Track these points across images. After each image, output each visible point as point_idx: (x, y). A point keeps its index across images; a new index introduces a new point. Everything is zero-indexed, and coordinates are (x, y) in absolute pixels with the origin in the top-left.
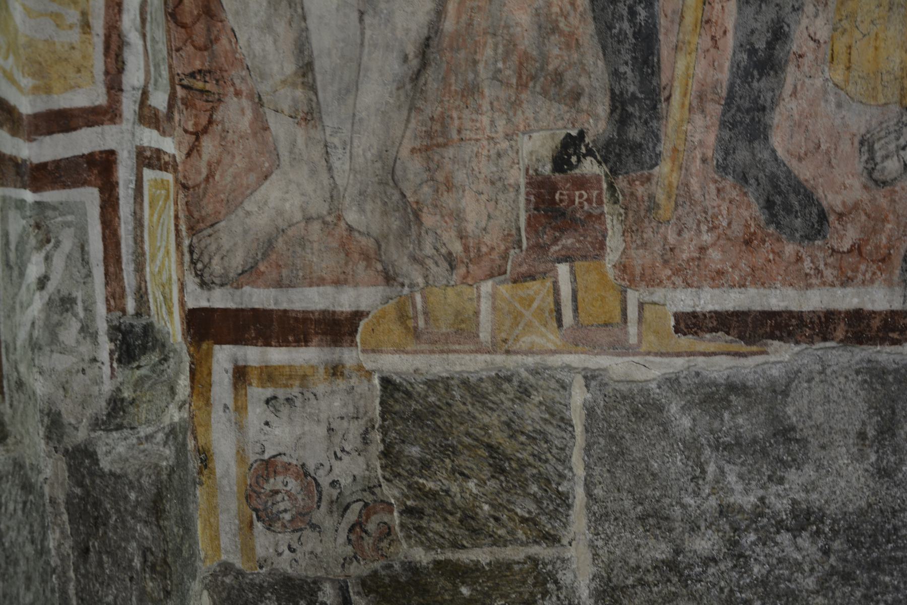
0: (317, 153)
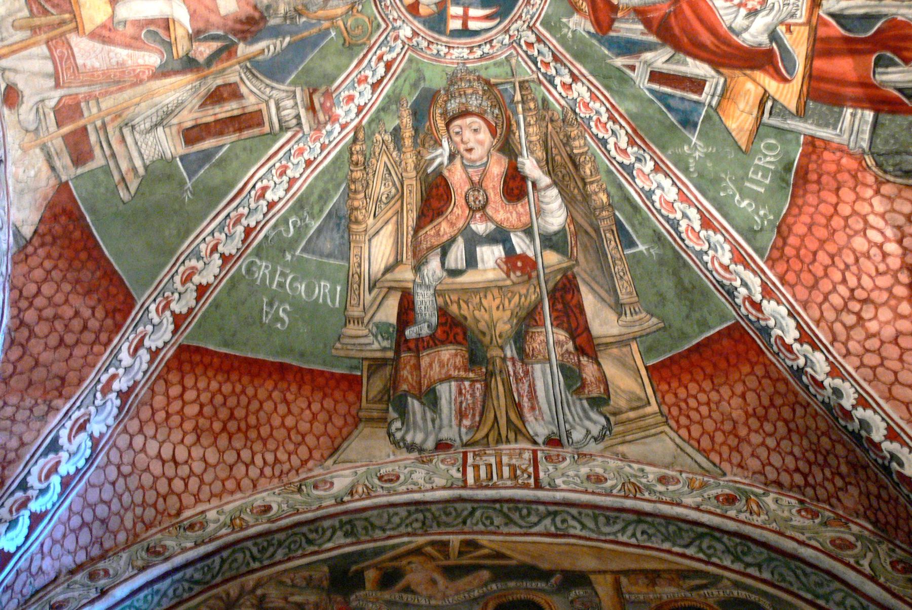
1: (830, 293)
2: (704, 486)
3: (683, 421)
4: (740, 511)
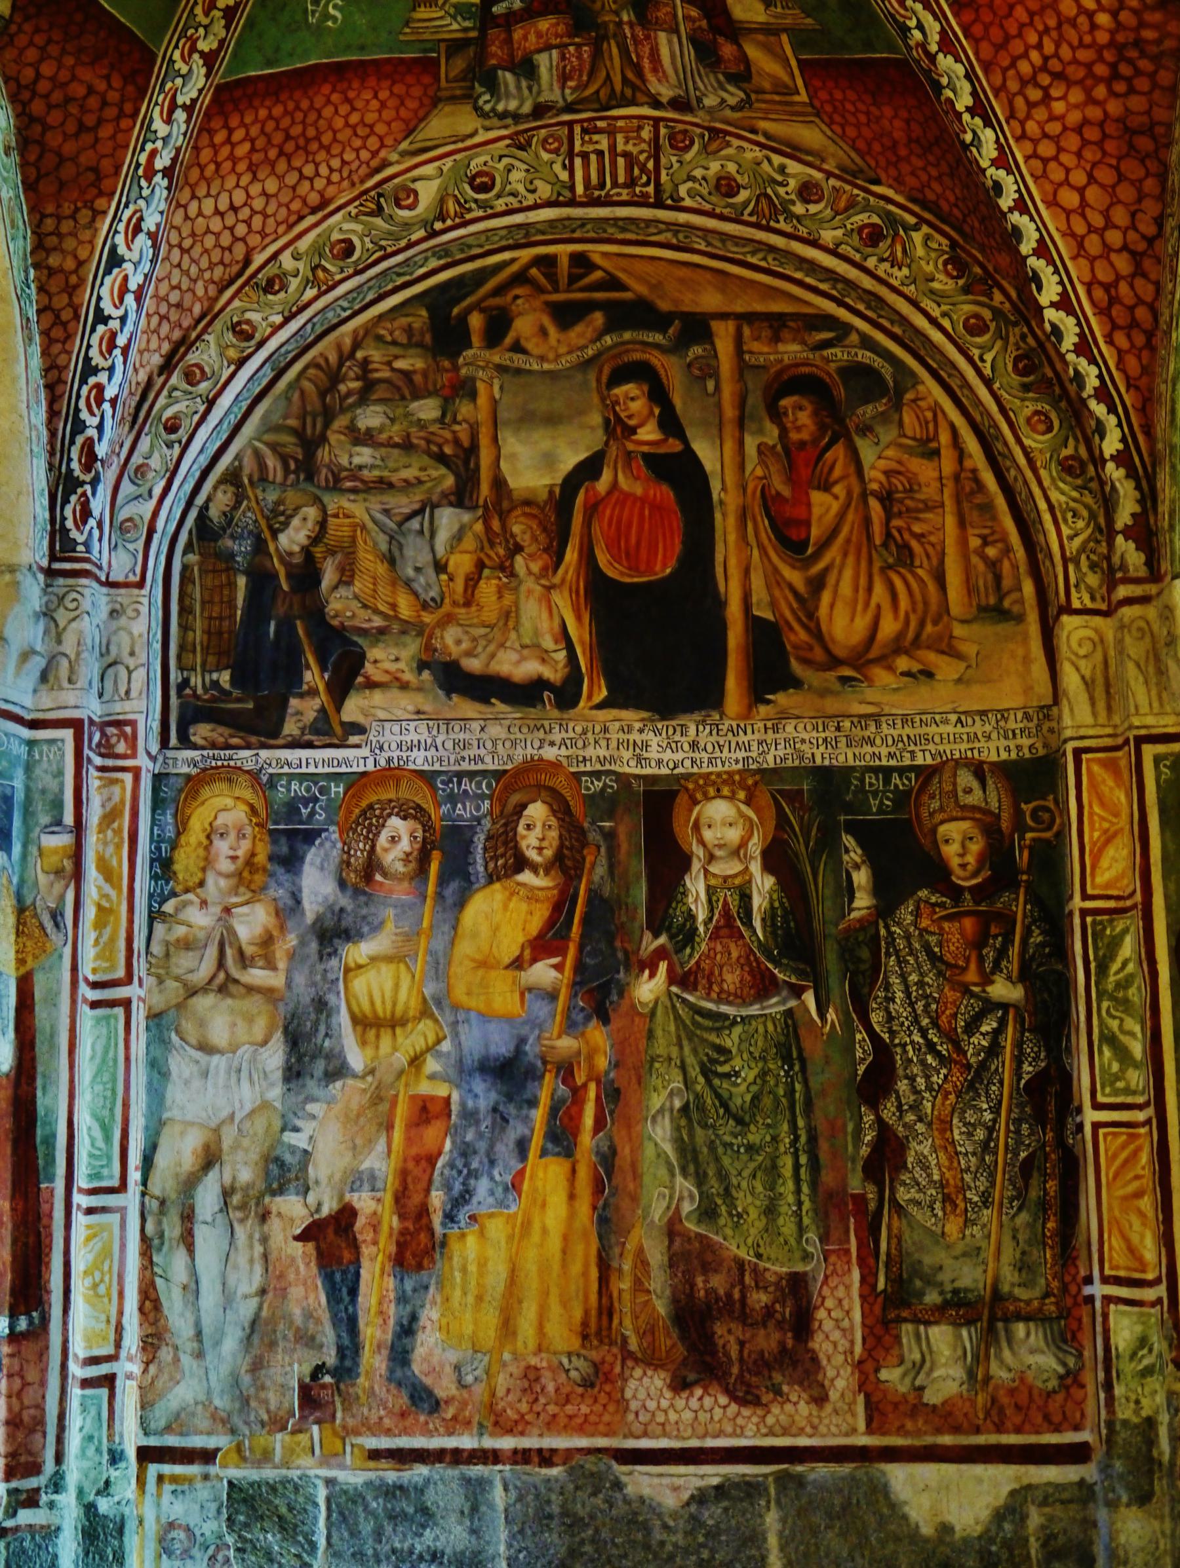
1: (1020, 57)
2: (852, 204)
3: (837, 118)
4: (882, 260)
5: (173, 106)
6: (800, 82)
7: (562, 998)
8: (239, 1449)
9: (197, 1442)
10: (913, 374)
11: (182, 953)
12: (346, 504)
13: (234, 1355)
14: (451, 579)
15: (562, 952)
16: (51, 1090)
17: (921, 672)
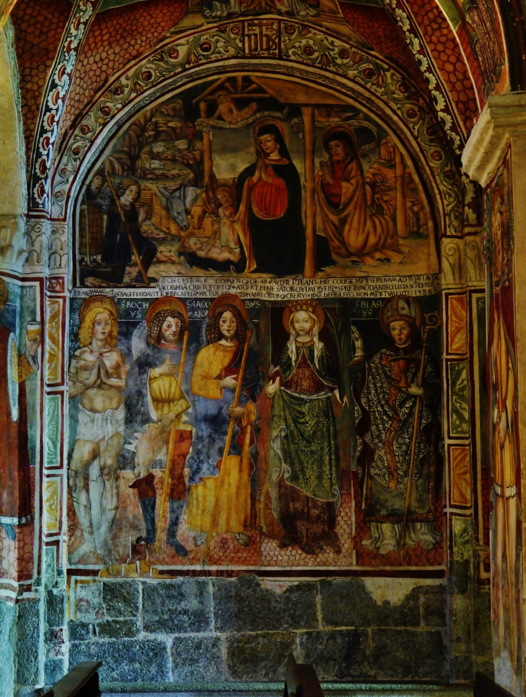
0: (92, 540)
4: (373, 84)
5: (79, 23)
6: (340, 10)
7: (237, 391)
8: (108, 570)
9: (91, 567)
10: (385, 131)
11: (83, 372)
12: (149, 185)
13: (105, 533)
14: (192, 217)
15: (237, 373)
16: (33, 428)
17: (385, 259)
